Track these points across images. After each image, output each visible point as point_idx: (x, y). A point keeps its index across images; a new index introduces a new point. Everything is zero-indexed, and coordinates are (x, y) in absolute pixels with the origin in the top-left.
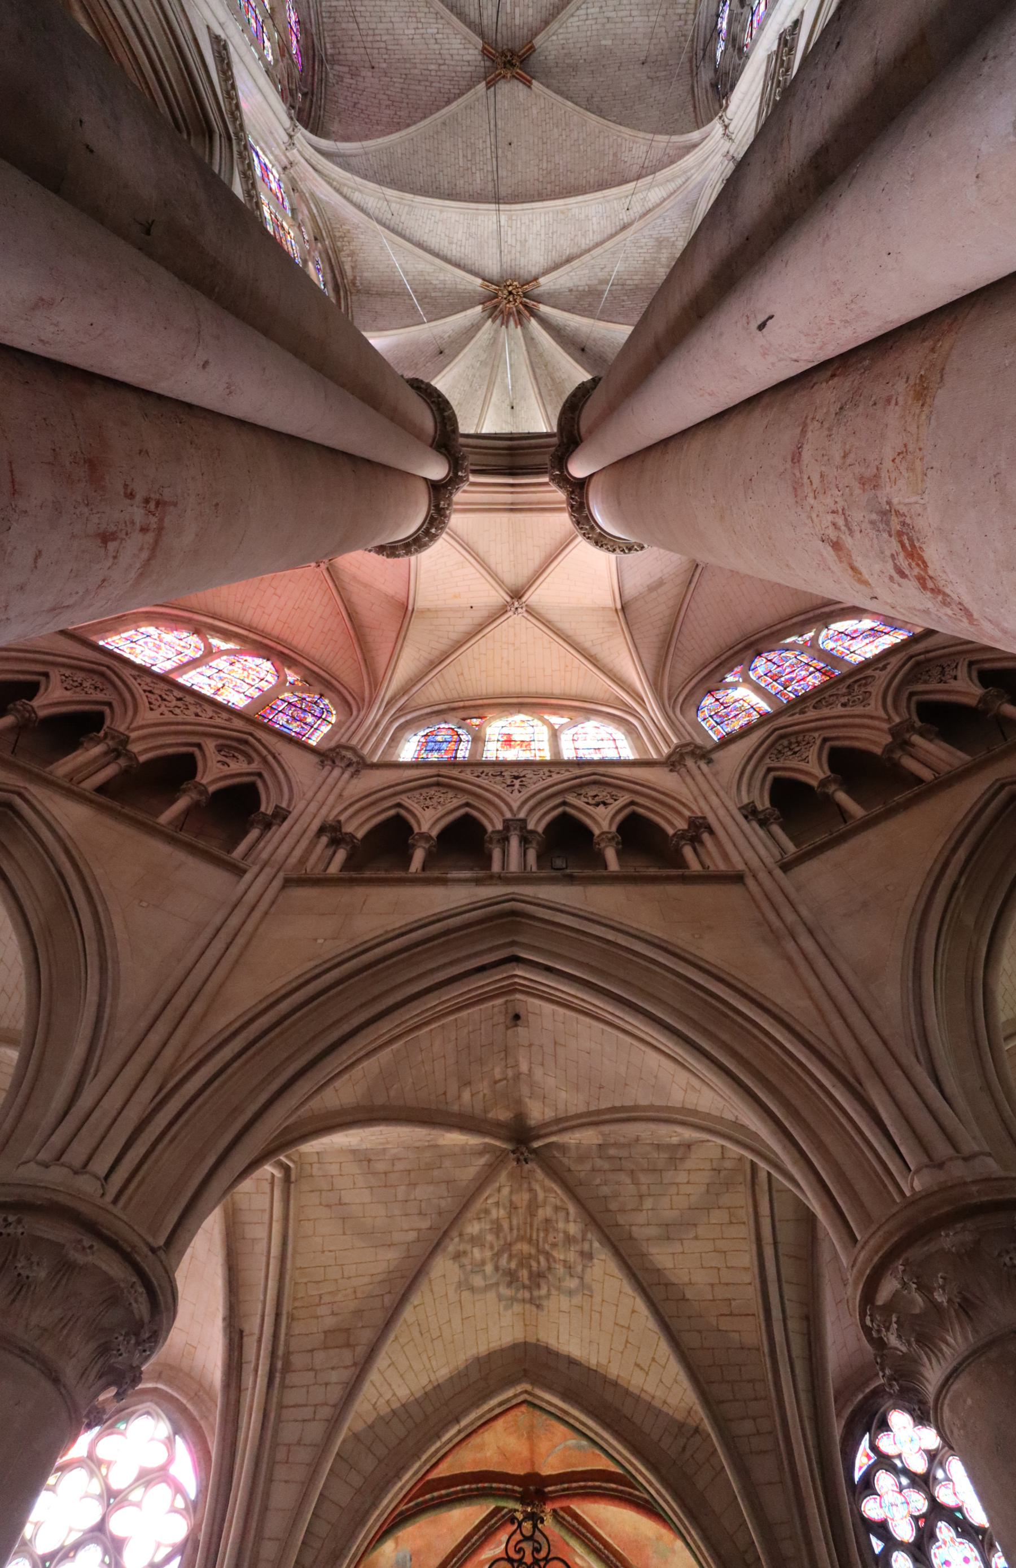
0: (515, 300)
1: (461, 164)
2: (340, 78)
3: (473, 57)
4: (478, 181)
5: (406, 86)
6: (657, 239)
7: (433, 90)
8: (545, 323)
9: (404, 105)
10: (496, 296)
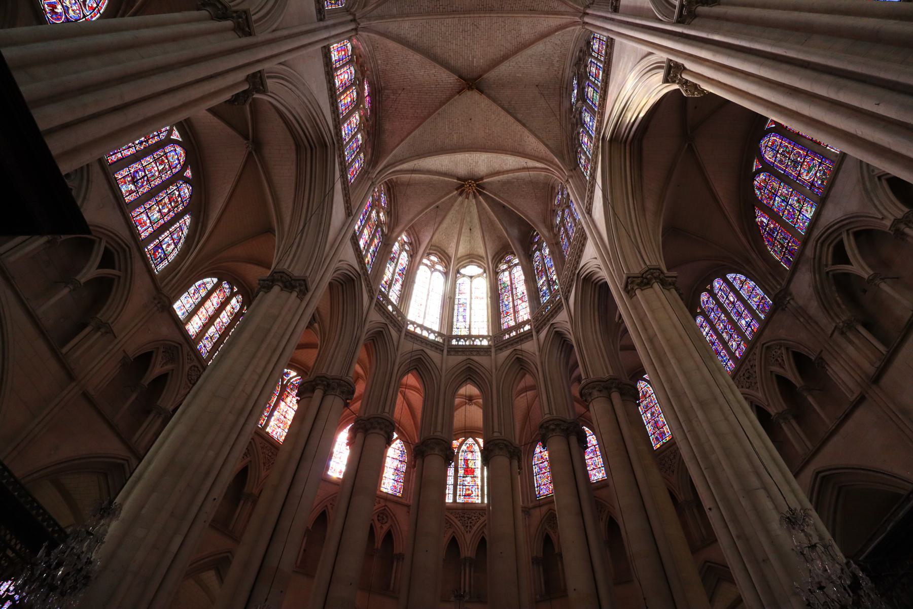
8: (487, 198)
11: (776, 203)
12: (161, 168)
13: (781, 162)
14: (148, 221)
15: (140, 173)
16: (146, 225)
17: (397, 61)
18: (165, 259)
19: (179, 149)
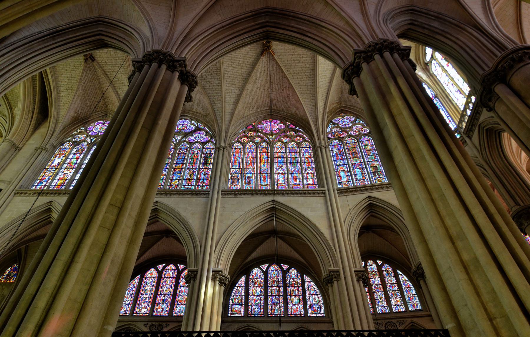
1: (301, 65)
2: (274, 105)
3: (265, 59)
4: (307, 58)
5: (275, 83)
7: (276, 73)
9: (282, 84)
12: (276, 285)
14: (297, 306)
16: (298, 309)
17: (251, 100)
18: (320, 305)
19: (272, 268)
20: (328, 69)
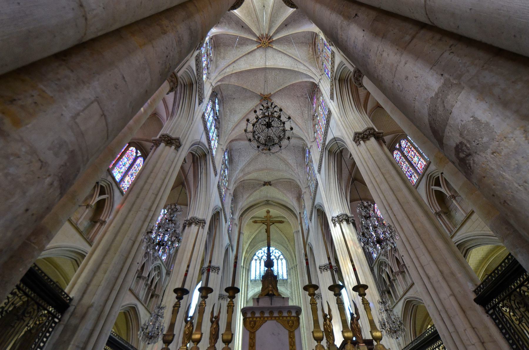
0: (263, 42)
6: (225, 59)
10: (269, 43)
11: (125, 158)
13: (135, 168)
15: (408, 174)
20: (281, 57)
